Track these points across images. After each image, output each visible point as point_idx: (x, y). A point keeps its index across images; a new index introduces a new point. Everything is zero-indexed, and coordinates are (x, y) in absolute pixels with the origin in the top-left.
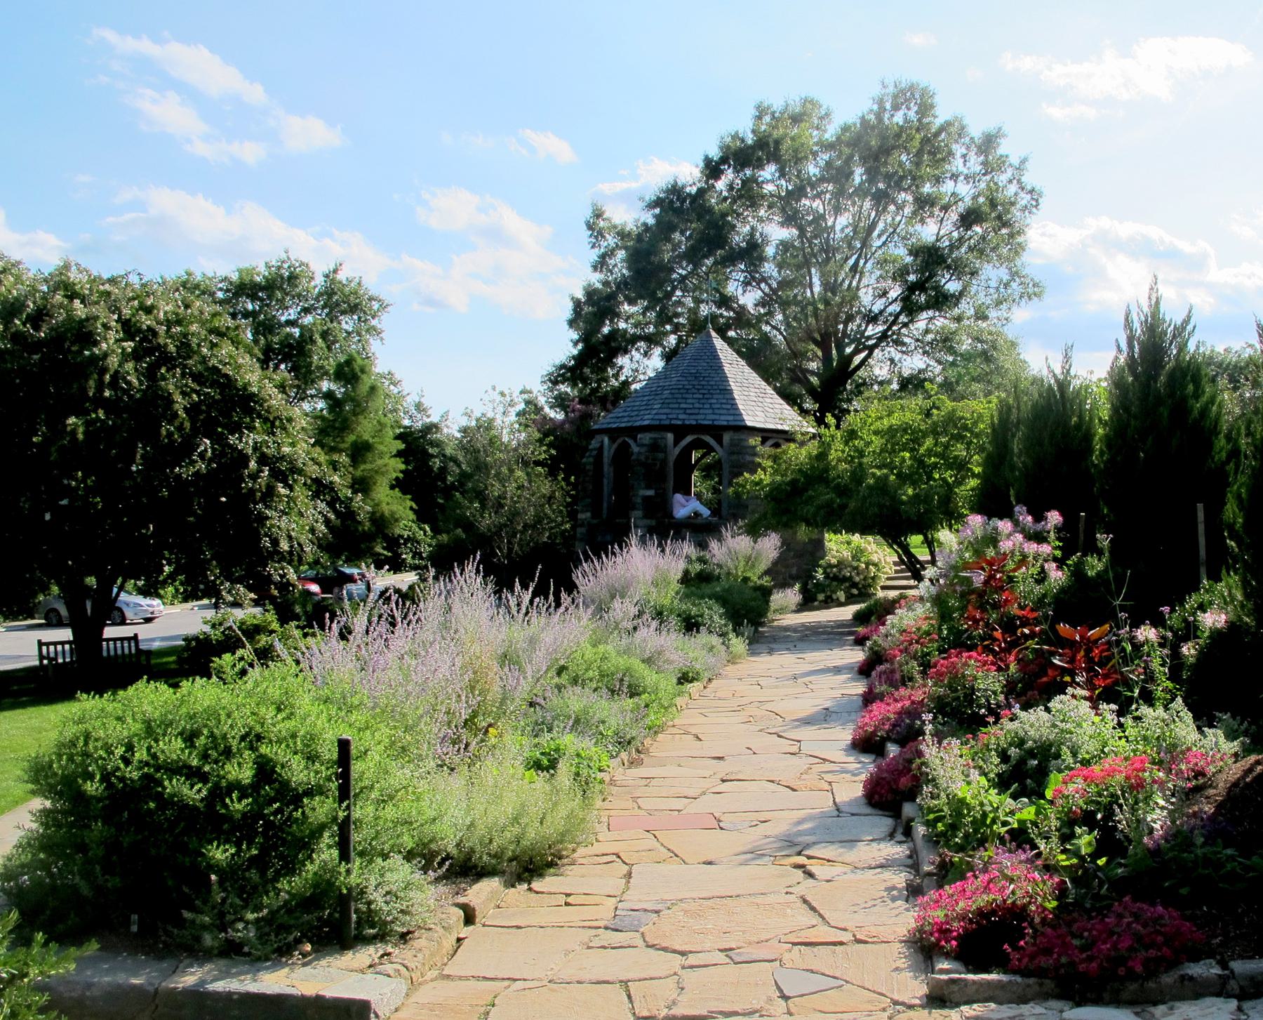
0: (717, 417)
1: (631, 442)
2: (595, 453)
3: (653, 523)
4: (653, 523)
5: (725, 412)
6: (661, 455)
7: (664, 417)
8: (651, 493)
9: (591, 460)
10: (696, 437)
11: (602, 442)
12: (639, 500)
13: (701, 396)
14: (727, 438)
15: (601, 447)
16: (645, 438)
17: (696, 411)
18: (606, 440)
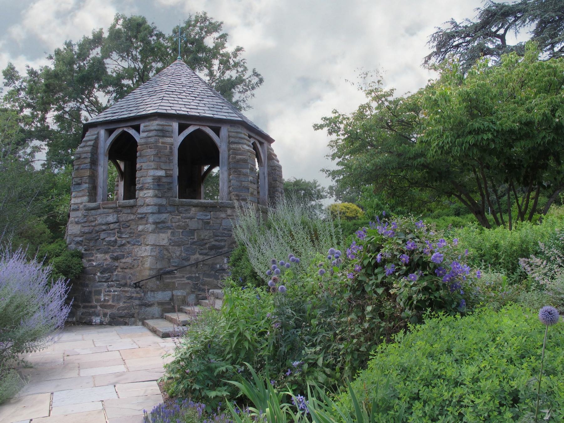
0: (215, 113)
1: (132, 132)
2: (91, 143)
3: (164, 201)
4: (164, 201)
5: (220, 110)
6: (168, 140)
7: (169, 108)
8: (161, 173)
9: (88, 149)
10: (197, 127)
11: (98, 134)
12: (149, 180)
13: (194, 98)
14: (224, 131)
15: (97, 140)
16: (155, 124)
17: (196, 107)
18: (102, 132)
